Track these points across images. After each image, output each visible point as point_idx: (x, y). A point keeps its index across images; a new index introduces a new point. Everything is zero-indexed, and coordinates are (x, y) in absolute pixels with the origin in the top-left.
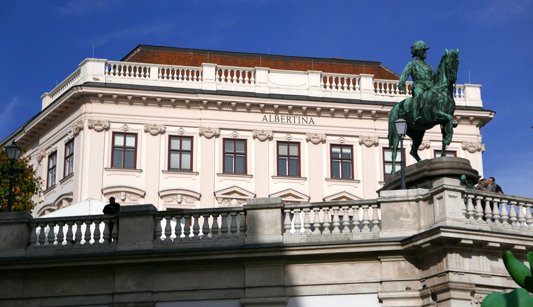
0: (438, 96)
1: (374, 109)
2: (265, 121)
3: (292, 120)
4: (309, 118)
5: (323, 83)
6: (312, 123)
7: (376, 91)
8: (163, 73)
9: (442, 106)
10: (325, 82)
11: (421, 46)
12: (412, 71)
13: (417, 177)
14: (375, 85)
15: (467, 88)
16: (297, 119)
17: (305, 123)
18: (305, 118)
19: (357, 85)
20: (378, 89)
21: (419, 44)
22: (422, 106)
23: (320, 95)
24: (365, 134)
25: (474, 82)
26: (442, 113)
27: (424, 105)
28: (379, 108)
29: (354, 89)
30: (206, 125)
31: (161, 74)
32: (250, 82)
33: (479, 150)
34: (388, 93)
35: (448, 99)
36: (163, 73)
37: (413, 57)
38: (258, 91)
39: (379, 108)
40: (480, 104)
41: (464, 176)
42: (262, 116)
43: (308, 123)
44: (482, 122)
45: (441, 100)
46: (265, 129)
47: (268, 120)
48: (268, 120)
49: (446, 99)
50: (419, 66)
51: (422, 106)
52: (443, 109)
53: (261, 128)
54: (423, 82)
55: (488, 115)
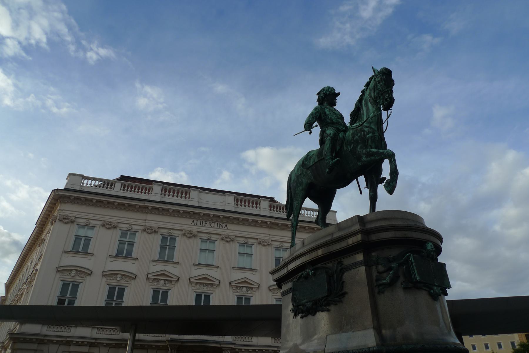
0: (364, 131)
1: (269, 220)
2: (193, 224)
3: (212, 225)
7: (271, 210)
8: (124, 187)
10: (237, 202)
11: (330, 90)
12: (320, 115)
14: (270, 206)
16: (216, 225)
17: (221, 227)
19: (258, 206)
20: (272, 209)
22: (338, 148)
23: (233, 209)
24: (262, 237)
26: (374, 150)
27: (341, 147)
28: (272, 220)
30: (148, 224)
31: (122, 188)
32: (186, 198)
34: (278, 212)
35: (379, 135)
36: (124, 187)
37: (310, 133)
38: (190, 203)
39: (272, 220)
41: (430, 244)
42: (191, 221)
45: (370, 135)
46: (192, 229)
47: (195, 223)
48: (195, 223)
49: (377, 134)
50: (330, 109)
51: (338, 148)
52: (373, 146)
53: (189, 229)
54: (335, 126)
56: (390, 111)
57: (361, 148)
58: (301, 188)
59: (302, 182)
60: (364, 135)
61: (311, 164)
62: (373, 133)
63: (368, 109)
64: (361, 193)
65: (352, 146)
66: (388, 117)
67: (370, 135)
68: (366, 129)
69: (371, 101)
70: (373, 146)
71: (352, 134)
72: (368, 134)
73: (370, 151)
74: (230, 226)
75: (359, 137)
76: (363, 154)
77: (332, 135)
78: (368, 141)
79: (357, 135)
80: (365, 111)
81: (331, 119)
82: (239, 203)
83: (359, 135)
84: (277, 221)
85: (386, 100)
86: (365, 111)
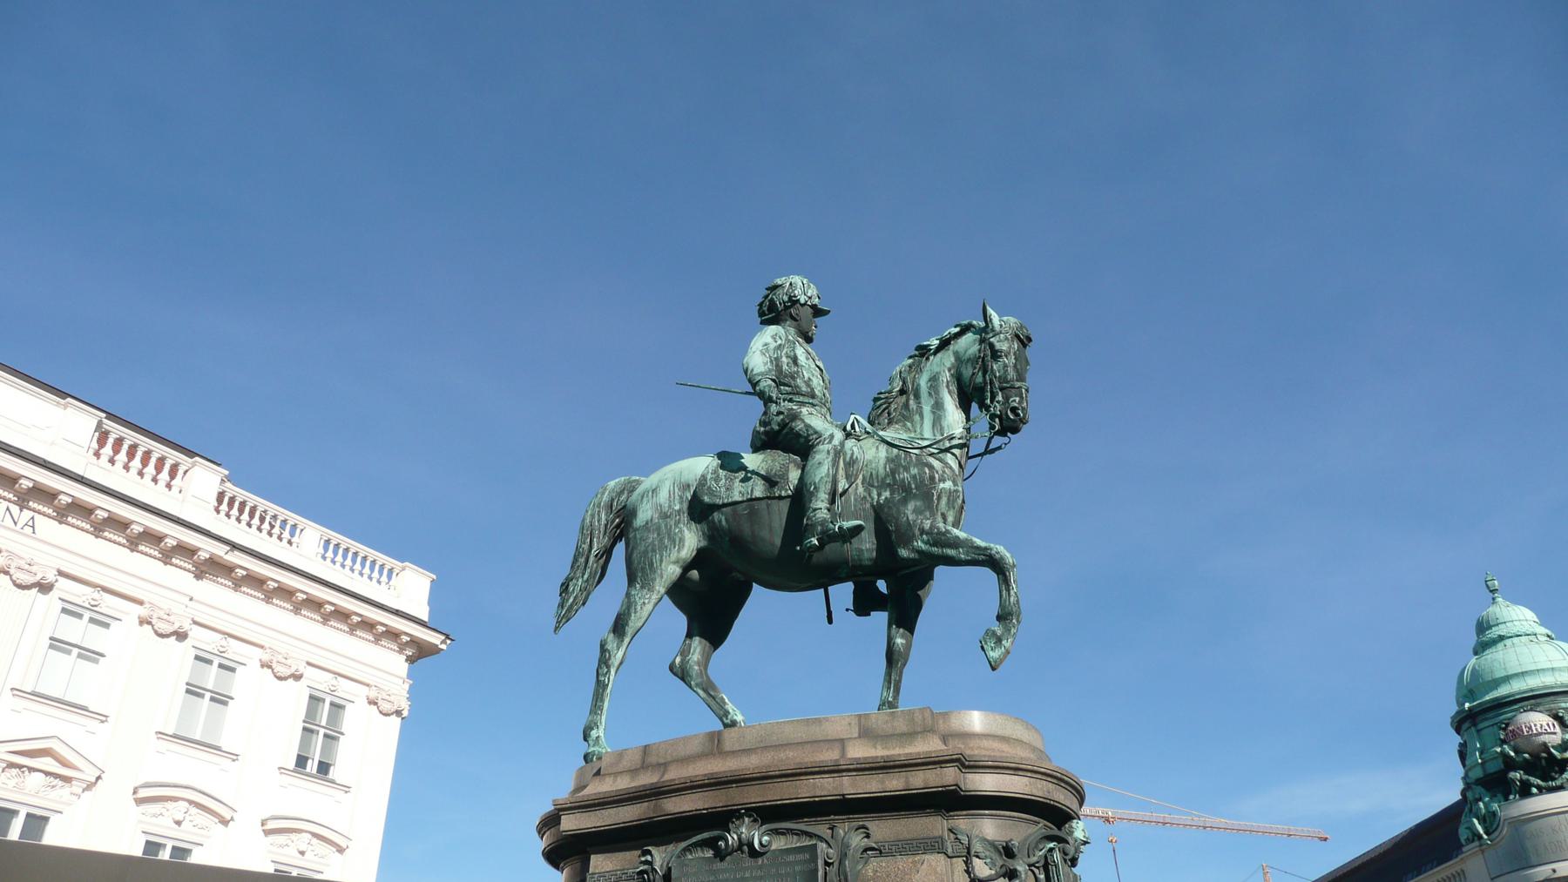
0: (931, 467)
4: (27, 514)
5: (95, 445)
6: (28, 530)
9: (951, 504)
13: (893, 784)
14: (220, 497)
15: (407, 573)
17: (8, 522)
18: (15, 509)
21: (803, 288)
25: (423, 563)
28: (220, 550)
29: (169, 486)
33: (398, 713)
39: (220, 550)
40: (424, 615)
43: (20, 524)
44: (420, 652)
45: (948, 485)
52: (950, 519)
55: (437, 642)
56: (998, 441)
57: (915, 511)
58: (674, 556)
59: (682, 540)
60: (932, 478)
61: (737, 498)
62: (955, 483)
63: (938, 406)
64: (830, 621)
65: (887, 494)
66: (988, 451)
67: (948, 485)
68: (936, 464)
69: (954, 388)
70: (950, 519)
71: (889, 460)
72: (943, 480)
73: (947, 531)
74: (47, 526)
75: (914, 477)
76: (922, 531)
77: (836, 442)
78: (939, 498)
79: (906, 469)
80: (927, 409)
81: (808, 383)
82: (107, 450)
83: (914, 471)
84: (236, 558)
85: (1014, 410)
86: (927, 409)
